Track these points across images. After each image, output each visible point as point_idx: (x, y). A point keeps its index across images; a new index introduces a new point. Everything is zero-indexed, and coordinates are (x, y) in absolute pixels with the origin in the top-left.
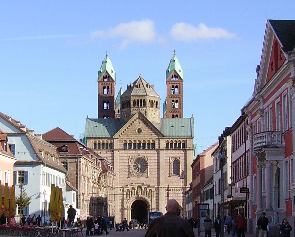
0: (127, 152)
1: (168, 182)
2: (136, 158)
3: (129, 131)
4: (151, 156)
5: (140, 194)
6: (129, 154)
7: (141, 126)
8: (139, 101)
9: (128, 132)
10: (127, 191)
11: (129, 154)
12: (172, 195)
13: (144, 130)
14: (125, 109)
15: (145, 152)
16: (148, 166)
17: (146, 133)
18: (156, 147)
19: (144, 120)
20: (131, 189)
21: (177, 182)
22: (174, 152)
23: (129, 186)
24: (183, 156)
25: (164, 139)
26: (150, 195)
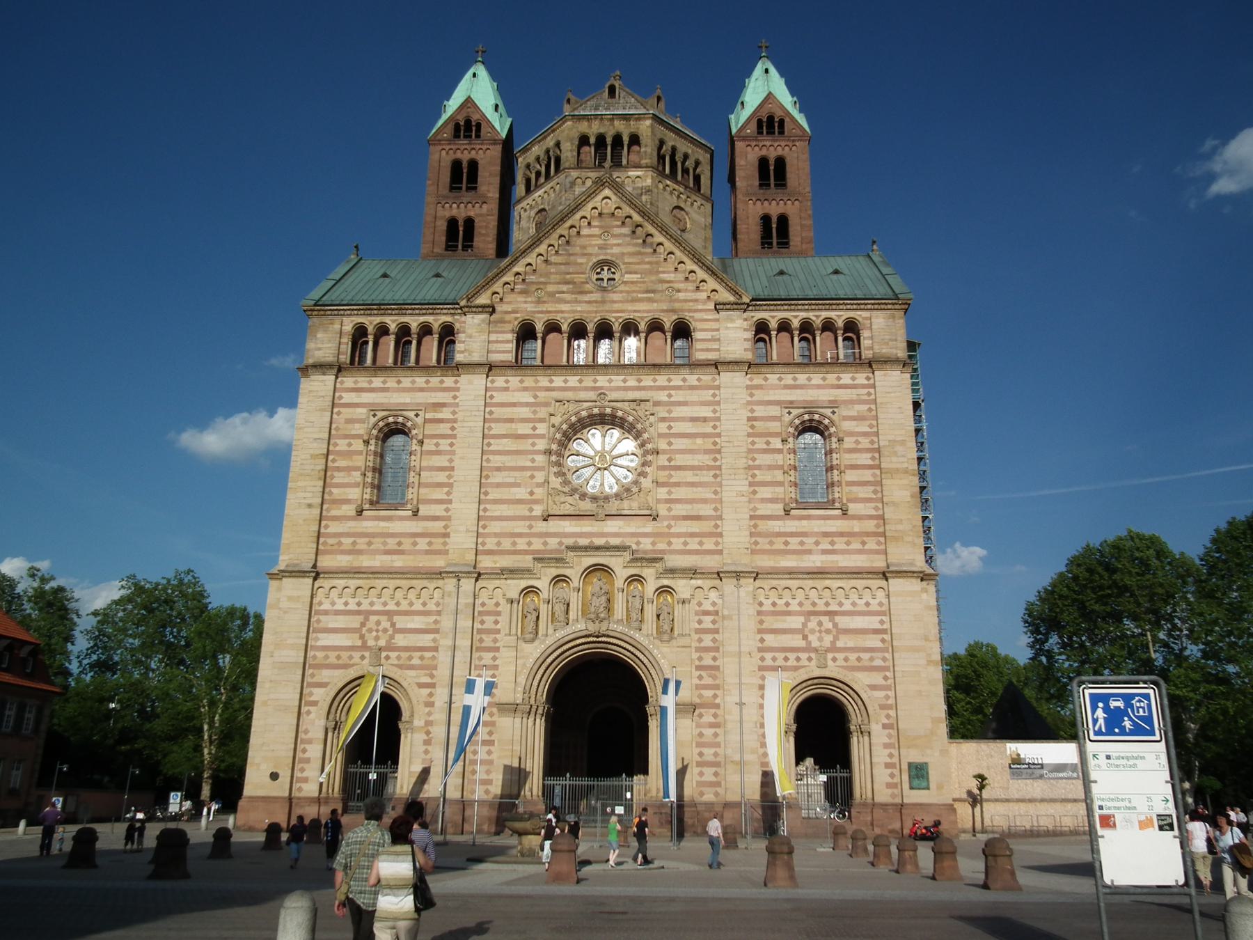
0: (536, 381)
1: (775, 547)
2: (584, 414)
3: (548, 274)
4: (672, 399)
6: (548, 389)
7: (616, 250)
8: (609, 140)
9: (542, 280)
11: (548, 389)
13: (637, 266)
14: (540, 192)
15: (640, 381)
17: (643, 287)
19: (630, 217)
21: (830, 547)
22: (802, 378)
24: (852, 402)
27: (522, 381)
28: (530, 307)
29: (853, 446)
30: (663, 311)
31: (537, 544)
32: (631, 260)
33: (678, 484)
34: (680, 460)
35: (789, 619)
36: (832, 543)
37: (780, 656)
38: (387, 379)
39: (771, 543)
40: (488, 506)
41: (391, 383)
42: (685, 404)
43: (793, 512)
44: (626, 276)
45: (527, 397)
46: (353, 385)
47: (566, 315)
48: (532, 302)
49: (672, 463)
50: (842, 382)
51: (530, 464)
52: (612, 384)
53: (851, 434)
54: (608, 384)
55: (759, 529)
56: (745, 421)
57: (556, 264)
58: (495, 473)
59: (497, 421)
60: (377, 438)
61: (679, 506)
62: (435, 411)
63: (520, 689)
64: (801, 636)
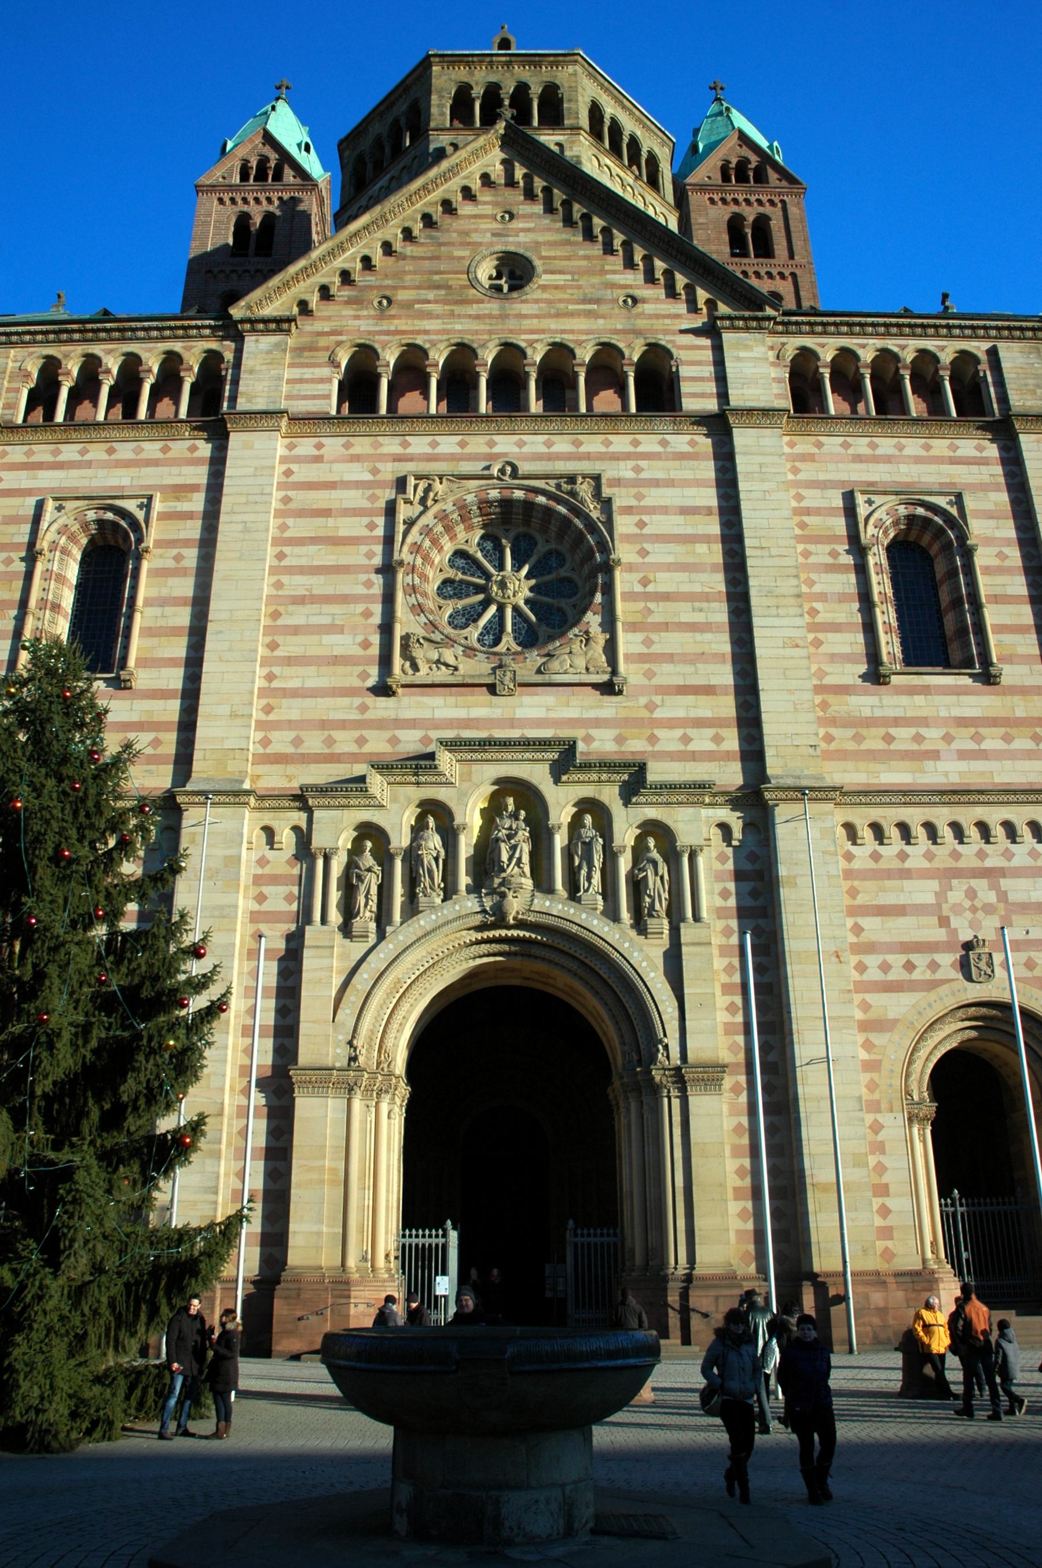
1: (864, 746)
2: (470, 498)
3: (399, 275)
4: (644, 475)
5: (528, 883)
7: (523, 238)
10: (356, 850)
11: (398, 459)
12: (930, 899)
15: (578, 444)
16: (608, 568)
17: (578, 294)
18: (689, 404)
20: (409, 817)
21: (972, 746)
22: (886, 445)
23: (376, 783)
24: (983, 488)
25: (770, 340)
26: (657, 884)
27: (347, 446)
28: (365, 325)
29: (997, 562)
30: (617, 332)
31: (378, 744)
32: (552, 254)
33: (665, 627)
34: (664, 582)
35: (907, 884)
36: (977, 738)
37: (897, 960)
38: (89, 446)
39: (858, 738)
40: (277, 670)
41: (97, 452)
42: (670, 483)
43: (895, 679)
44: (544, 277)
45: (359, 473)
46: (25, 459)
47: (434, 337)
48: (369, 317)
49: (650, 588)
50: (959, 453)
51: (365, 591)
52: (525, 449)
53: (989, 541)
54: (516, 450)
55: (831, 712)
56: (788, 513)
57: (413, 258)
58: (291, 608)
59: (302, 513)
60: (65, 552)
61: (667, 668)
62: (178, 499)
63: (344, 1037)
64: (935, 920)
